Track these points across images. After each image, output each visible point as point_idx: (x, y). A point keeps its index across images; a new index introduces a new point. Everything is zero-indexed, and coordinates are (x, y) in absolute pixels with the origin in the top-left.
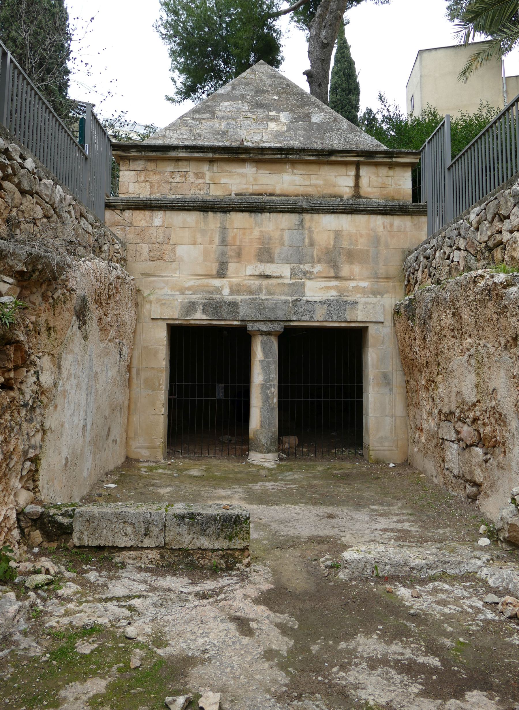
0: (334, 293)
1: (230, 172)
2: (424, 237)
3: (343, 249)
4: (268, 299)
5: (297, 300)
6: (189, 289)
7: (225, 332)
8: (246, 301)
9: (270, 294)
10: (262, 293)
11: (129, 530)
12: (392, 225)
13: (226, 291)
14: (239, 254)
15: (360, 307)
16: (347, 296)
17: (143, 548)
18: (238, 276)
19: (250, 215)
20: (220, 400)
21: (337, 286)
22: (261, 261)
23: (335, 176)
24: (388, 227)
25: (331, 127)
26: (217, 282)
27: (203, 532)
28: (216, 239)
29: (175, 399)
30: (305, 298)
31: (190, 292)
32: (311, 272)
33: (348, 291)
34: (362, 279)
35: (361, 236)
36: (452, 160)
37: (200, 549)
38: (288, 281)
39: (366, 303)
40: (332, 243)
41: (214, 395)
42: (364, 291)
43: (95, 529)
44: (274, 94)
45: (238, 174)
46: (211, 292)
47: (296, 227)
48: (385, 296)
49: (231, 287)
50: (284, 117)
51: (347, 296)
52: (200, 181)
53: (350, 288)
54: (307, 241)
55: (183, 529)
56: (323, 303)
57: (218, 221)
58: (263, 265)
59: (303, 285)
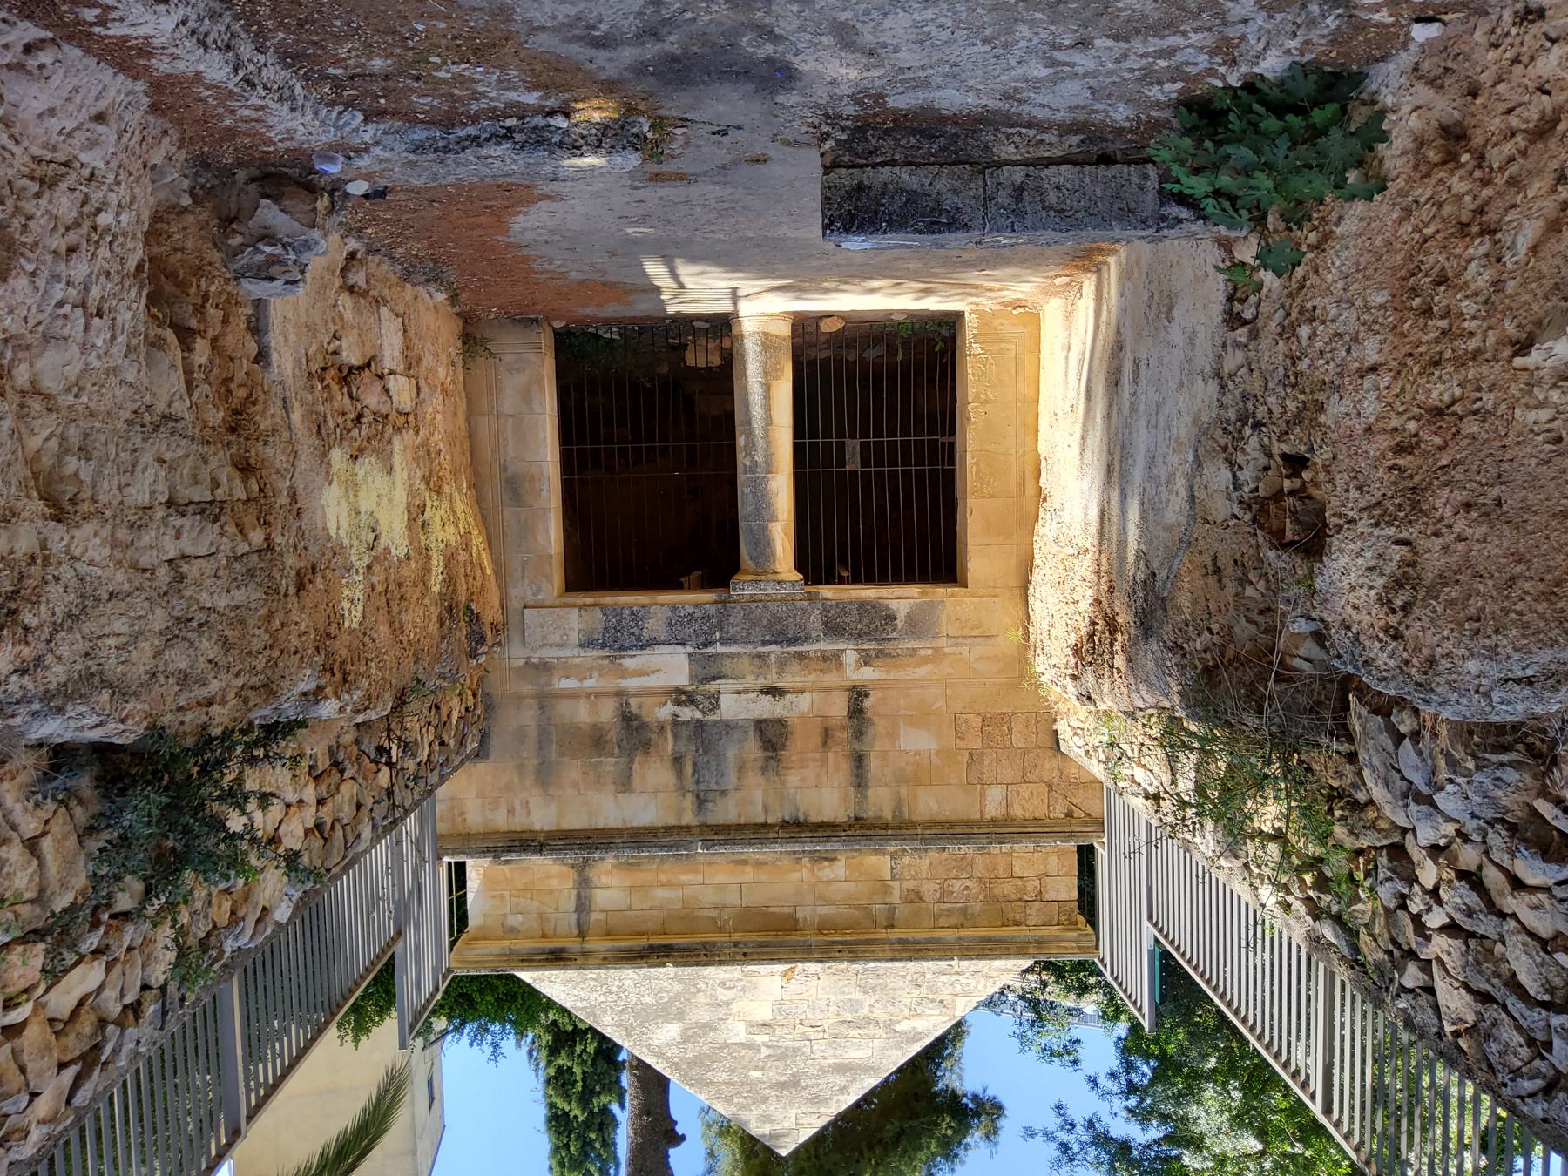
0: (629, 663)
1: (851, 906)
2: (441, 792)
3: (612, 755)
4: (764, 643)
5: (705, 646)
6: (926, 660)
7: (845, 574)
8: (808, 639)
9: (760, 656)
10: (778, 658)
11: (1052, 198)
12: (511, 811)
13: (850, 657)
14: (827, 734)
15: (574, 638)
16: (603, 658)
17: (1026, 163)
18: (828, 689)
19: (806, 816)
20: (853, 437)
21: (624, 677)
22: (781, 723)
23: (630, 909)
24: (518, 807)
25: (637, 1016)
26: (868, 674)
27: (913, 197)
28: (874, 764)
29: (943, 435)
30: (690, 650)
31: (922, 653)
32: (678, 703)
33: (600, 669)
34: (573, 695)
35: (575, 785)
36: (392, 956)
37: (918, 165)
38: (726, 686)
39: (562, 646)
40: (636, 767)
41: (864, 447)
42: (569, 670)
43: (1117, 196)
44: (759, 1081)
45: (832, 903)
46: (880, 654)
47: (711, 796)
48: (522, 662)
49: (840, 665)
50: (737, 1032)
51: (603, 658)
52: (910, 884)
53: (595, 674)
54: (689, 769)
55: (949, 201)
56: (653, 643)
57: (871, 800)
58: (777, 715)
59: (692, 678)
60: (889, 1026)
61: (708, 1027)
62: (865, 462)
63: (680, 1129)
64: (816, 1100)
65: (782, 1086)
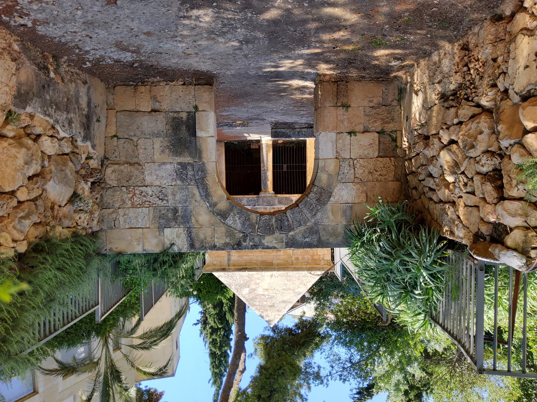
11: (304, 133)
27: (284, 133)
52: (296, 256)
60: (293, 290)
61: (254, 290)
62: (287, 169)
63: (247, 336)
64: (278, 311)
65: (271, 306)
